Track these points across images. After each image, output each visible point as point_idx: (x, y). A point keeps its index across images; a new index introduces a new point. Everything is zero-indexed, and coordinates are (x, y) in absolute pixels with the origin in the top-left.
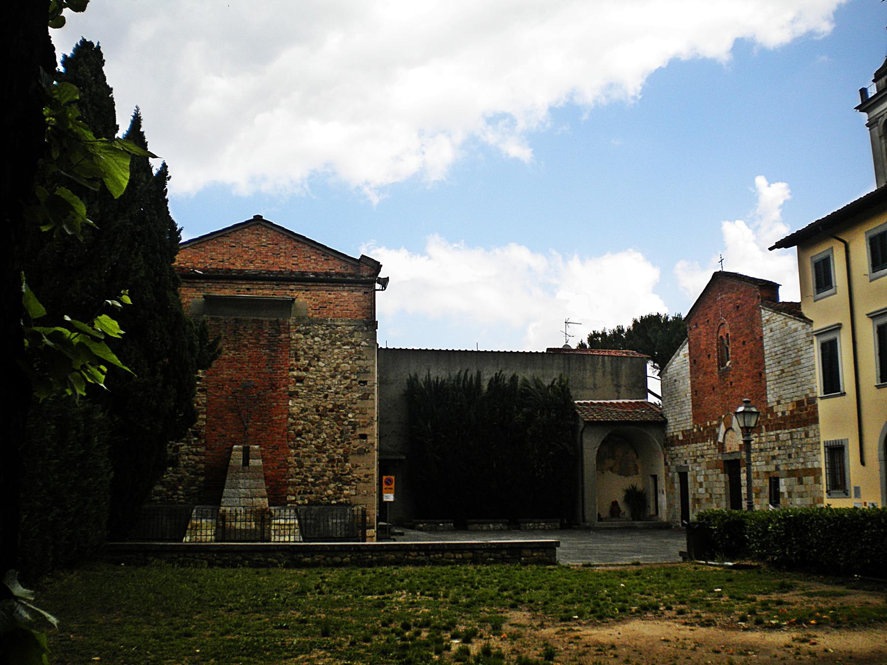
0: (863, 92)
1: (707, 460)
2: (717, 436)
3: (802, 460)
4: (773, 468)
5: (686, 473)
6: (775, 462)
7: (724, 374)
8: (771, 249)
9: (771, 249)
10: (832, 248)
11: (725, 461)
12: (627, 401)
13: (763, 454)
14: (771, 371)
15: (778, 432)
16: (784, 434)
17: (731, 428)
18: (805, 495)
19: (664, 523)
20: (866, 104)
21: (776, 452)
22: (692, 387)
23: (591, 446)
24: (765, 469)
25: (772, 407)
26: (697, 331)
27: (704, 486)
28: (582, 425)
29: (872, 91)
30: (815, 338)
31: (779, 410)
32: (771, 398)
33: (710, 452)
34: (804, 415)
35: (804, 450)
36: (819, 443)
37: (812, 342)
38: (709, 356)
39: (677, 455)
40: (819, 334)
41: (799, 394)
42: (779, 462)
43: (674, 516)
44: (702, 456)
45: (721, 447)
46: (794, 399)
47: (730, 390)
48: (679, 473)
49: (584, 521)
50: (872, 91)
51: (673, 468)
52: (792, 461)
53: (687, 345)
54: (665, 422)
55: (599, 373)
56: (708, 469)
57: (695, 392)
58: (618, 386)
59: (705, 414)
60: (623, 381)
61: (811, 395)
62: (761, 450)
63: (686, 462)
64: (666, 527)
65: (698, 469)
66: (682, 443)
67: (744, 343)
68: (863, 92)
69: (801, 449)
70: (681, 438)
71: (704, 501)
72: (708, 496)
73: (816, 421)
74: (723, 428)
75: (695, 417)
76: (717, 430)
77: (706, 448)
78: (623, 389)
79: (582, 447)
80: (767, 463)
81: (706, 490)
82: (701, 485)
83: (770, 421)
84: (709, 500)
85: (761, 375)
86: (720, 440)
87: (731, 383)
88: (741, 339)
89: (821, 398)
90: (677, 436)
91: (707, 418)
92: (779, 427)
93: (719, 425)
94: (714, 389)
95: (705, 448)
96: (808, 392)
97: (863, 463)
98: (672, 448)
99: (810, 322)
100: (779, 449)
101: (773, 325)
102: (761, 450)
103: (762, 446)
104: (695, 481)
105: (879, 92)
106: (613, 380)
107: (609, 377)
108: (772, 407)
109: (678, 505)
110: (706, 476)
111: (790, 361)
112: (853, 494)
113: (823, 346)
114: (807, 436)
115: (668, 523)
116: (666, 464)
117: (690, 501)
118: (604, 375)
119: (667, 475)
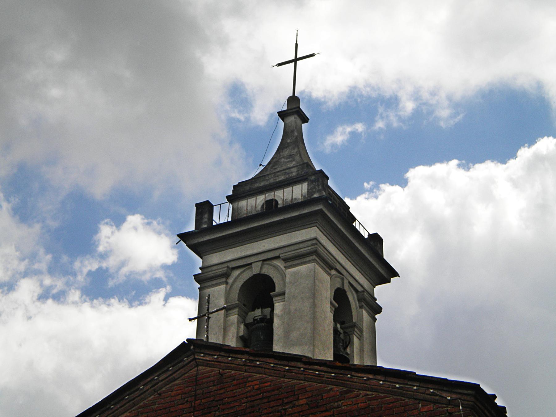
0: (204, 209)
29: (222, 215)
50: (222, 215)
68: (204, 209)
105: (236, 221)
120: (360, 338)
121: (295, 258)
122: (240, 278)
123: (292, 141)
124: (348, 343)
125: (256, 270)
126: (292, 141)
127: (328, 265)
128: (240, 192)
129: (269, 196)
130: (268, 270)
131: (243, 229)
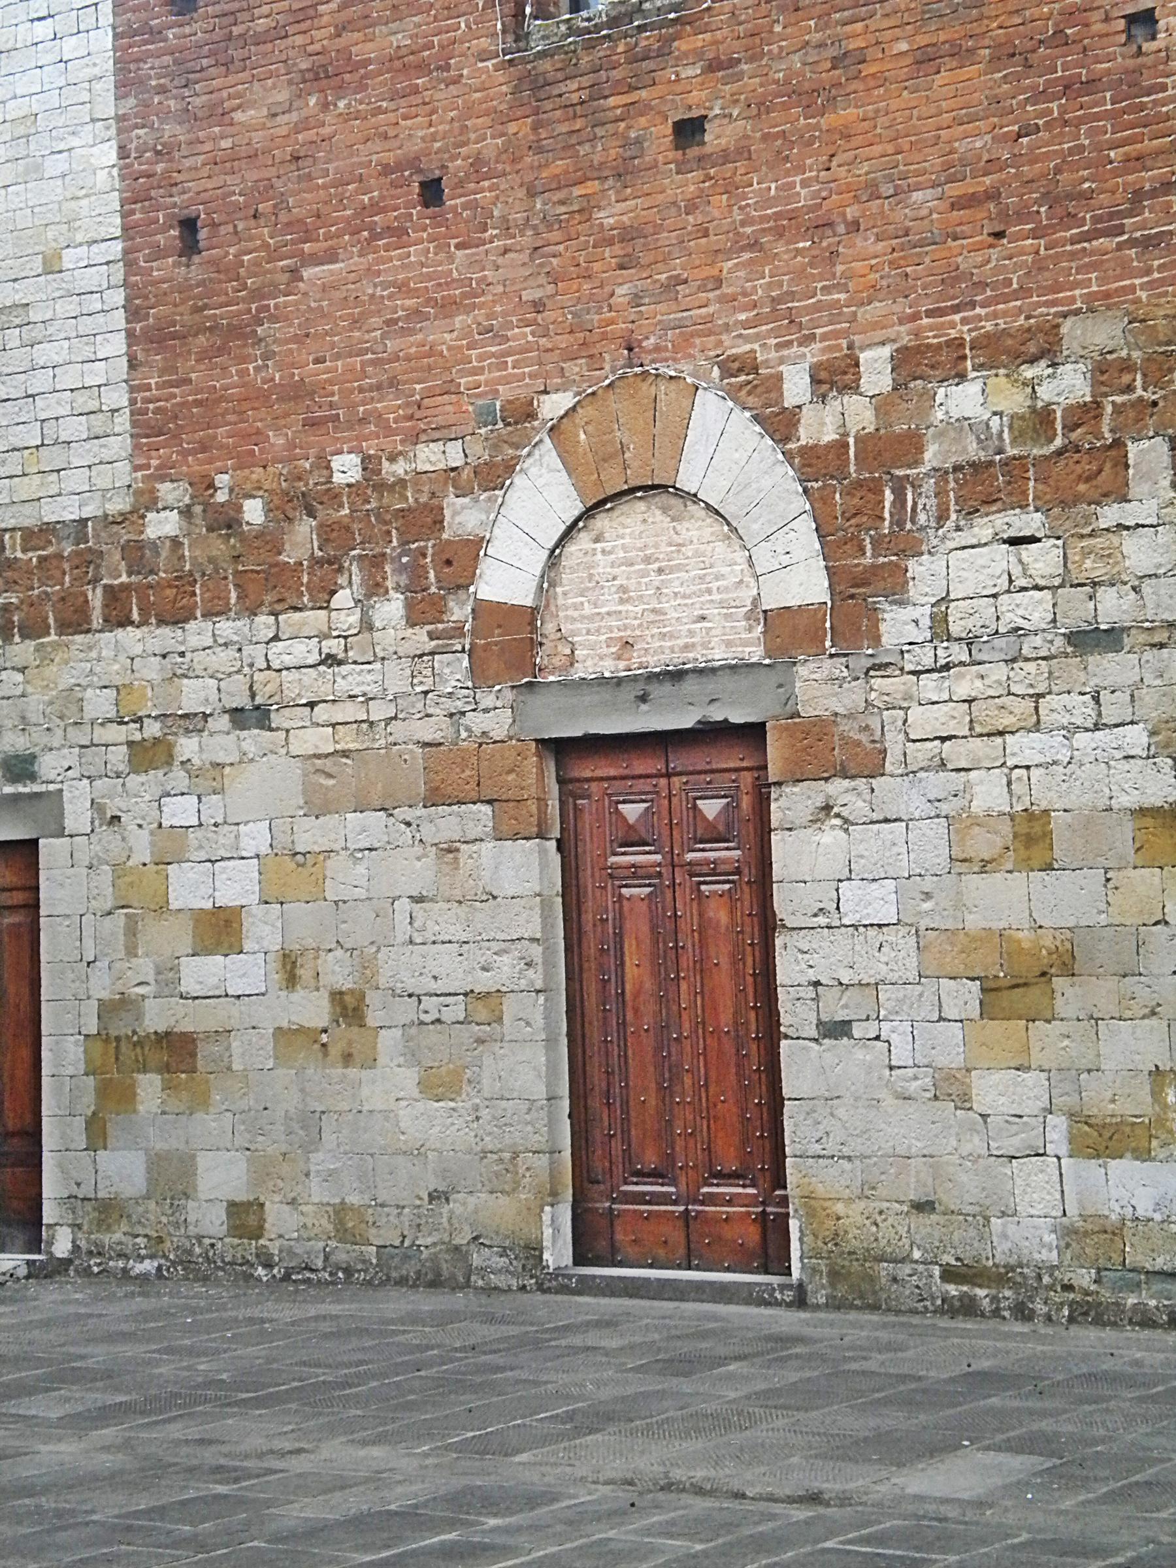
13: (1111, 668)
22: (138, 192)
27: (264, 932)
33: (351, 679)
44: (252, 716)
56: (319, 806)
59: (298, 392)
62: (1091, 640)
71: (249, 1052)
72: (311, 1009)
76: (463, 516)
81: (290, 969)
82: (220, 930)
86: (506, 579)
87: (689, 131)
93: (494, 476)
94: (432, 192)
95: (304, 651)
102: (1091, 640)
103: (1112, 607)
104: (137, 903)
110: (293, 870)
117: (63, 1054)
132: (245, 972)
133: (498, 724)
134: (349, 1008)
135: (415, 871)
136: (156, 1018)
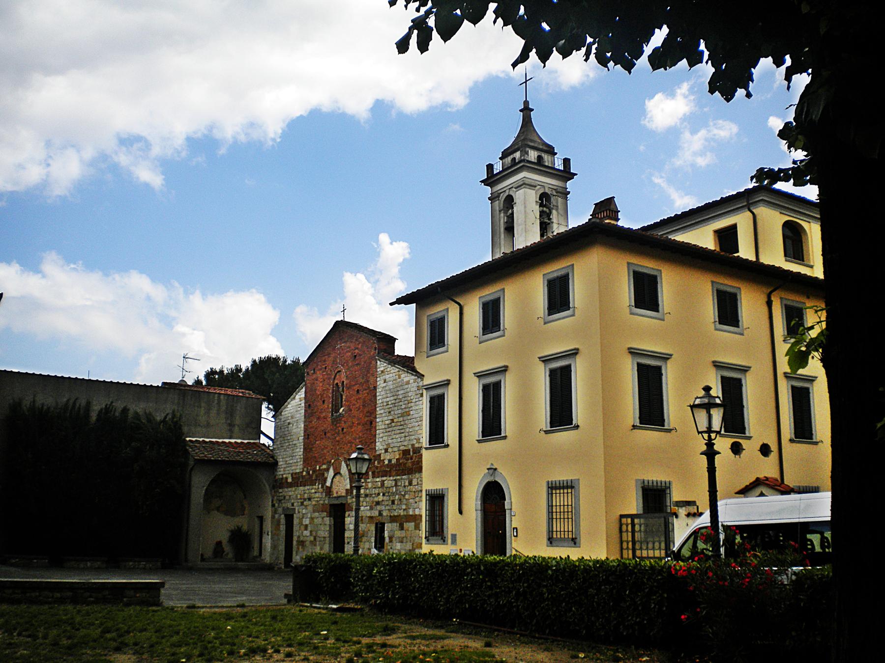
0: (490, 167)
1: (314, 503)
2: (325, 480)
3: (404, 507)
4: (377, 513)
5: (292, 516)
6: (379, 508)
7: (336, 420)
8: (391, 304)
9: (391, 304)
10: (448, 309)
11: (331, 505)
12: (239, 441)
13: (368, 499)
14: (382, 420)
15: (384, 478)
16: (389, 481)
17: (339, 473)
18: (405, 540)
19: (266, 565)
20: (491, 179)
21: (381, 498)
22: (305, 430)
23: (199, 484)
24: (369, 514)
25: (380, 455)
26: (315, 376)
27: (309, 529)
28: (191, 463)
29: (498, 168)
30: (425, 392)
31: (386, 458)
32: (379, 446)
33: (317, 495)
34: (409, 464)
35: (407, 496)
36: (421, 491)
37: (422, 395)
38: (324, 402)
39: (285, 497)
40: (429, 388)
41: (406, 443)
42: (383, 508)
43: (277, 558)
44: (309, 499)
45: (329, 491)
46: (402, 448)
47: (342, 436)
48: (286, 516)
49: (186, 560)
50: (498, 168)
51: (280, 510)
52: (395, 507)
53: (304, 390)
54: (276, 464)
55: (214, 412)
56: (314, 511)
57: (307, 436)
58: (231, 425)
60: (238, 420)
61: (417, 445)
63: (293, 505)
64: (269, 568)
65: (304, 511)
66: (290, 485)
67: (358, 391)
68: (490, 167)
69: (404, 496)
70: (290, 480)
71: (307, 543)
72: (312, 539)
73: (420, 470)
74: (331, 473)
75: (306, 460)
77: (315, 491)
78: (236, 429)
79: (190, 485)
80: (371, 508)
83: (377, 468)
84: (313, 543)
85: (371, 423)
86: (328, 484)
88: (356, 388)
89: (426, 449)
90: (287, 478)
91: (317, 462)
92: (385, 474)
93: (328, 470)
95: (313, 491)
96: (415, 442)
97: (461, 512)
98: (281, 490)
99: (421, 376)
100: (384, 495)
101: (387, 377)
104: (301, 523)
106: (227, 419)
107: (223, 416)
108: (380, 455)
109: (282, 547)
110: (312, 519)
111: (400, 411)
112: (450, 541)
113: (432, 400)
114: (410, 484)
115: (271, 564)
116: (273, 505)
117: (295, 543)
118: (218, 414)
119: (273, 517)
120: (557, 210)
121: (518, 187)
122: (503, 197)
123: (527, 122)
124: (549, 215)
125: (507, 194)
126: (527, 122)
127: (532, 186)
128: (505, 154)
129: (512, 156)
130: (511, 193)
131: (507, 172)
132: (307, 533)
133: (326, 502)
134: (315, 539)
135: (320, 520)
136: (302, 539)
